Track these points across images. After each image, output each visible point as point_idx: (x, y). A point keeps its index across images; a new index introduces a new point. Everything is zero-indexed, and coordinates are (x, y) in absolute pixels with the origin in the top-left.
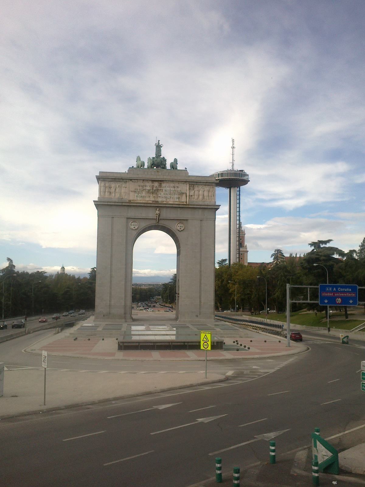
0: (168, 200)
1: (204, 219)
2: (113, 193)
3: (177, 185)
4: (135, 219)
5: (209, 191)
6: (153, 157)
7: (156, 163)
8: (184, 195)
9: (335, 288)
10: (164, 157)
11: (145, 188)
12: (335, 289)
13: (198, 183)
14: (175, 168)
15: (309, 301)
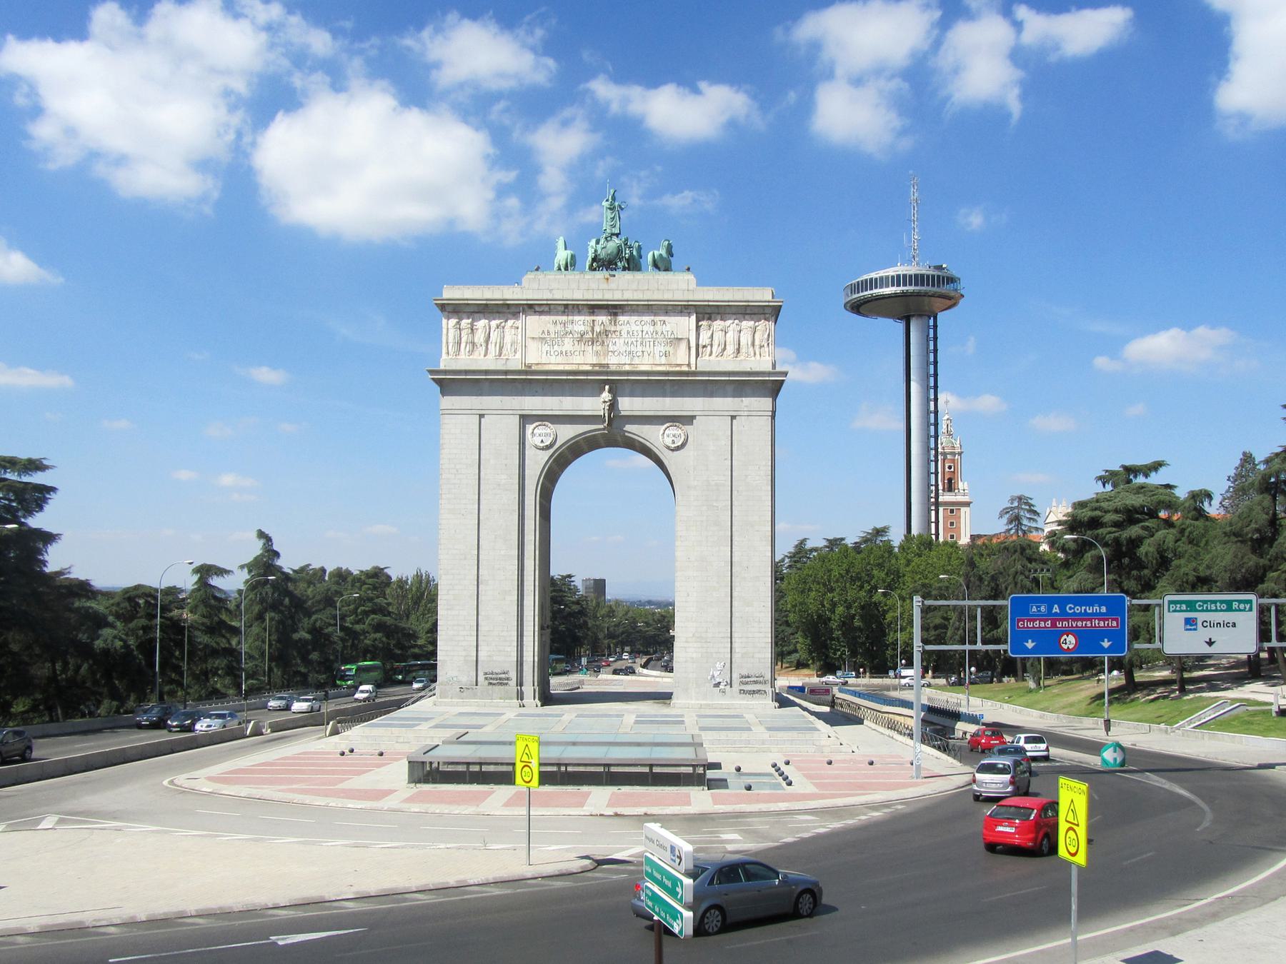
0: (636, 361)
1: (742, 413)
8: (684, 345)
9: (1056, 606)
11: (570, 327)
12: (1056, 609)
15: (979, 646)
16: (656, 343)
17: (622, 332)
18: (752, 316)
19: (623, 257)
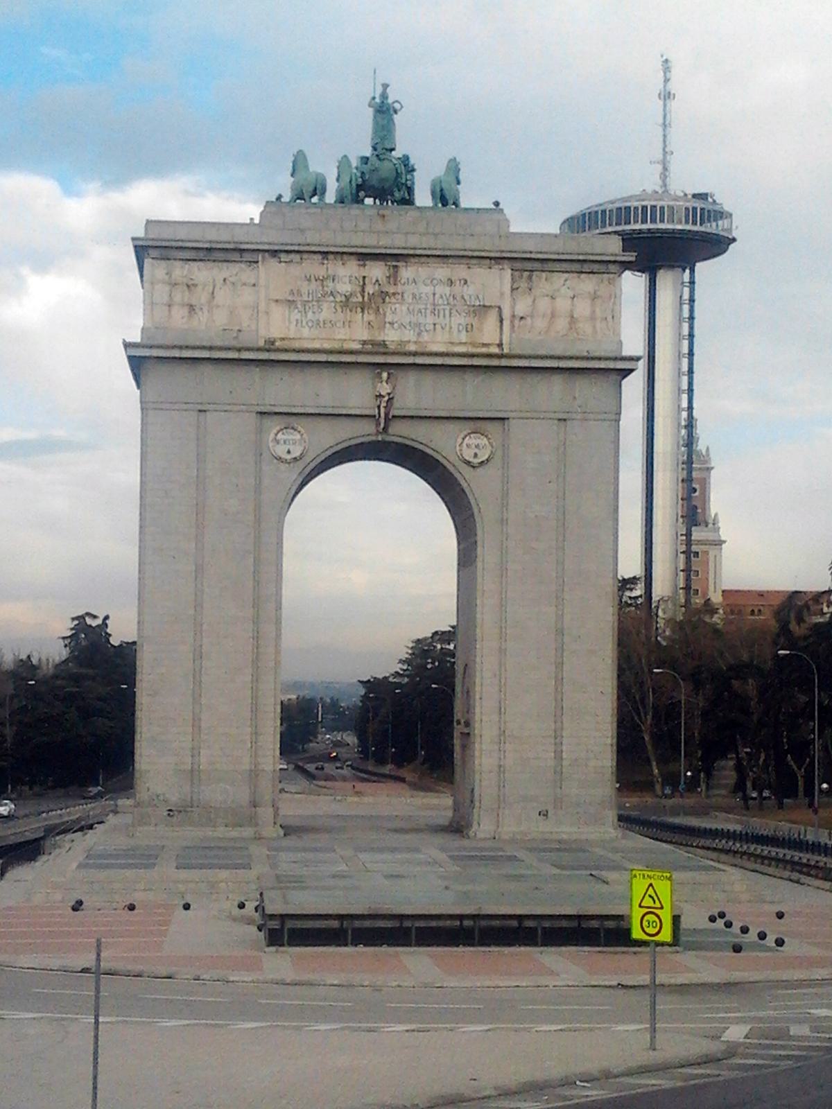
0: (425, 337)
1: (574, 416)
2: (201, 309)
3: (460, 271)
4: (290, 416)
5: (594, 297)
6: (362, 158)
7: (374, 182)
8: (492, 318)
10: (405, 160)
13: (550, 266)
14: (451, 202)
16: (454, 312)
17: (405, 295)
18: (591, 275)
19: (403, 184)
